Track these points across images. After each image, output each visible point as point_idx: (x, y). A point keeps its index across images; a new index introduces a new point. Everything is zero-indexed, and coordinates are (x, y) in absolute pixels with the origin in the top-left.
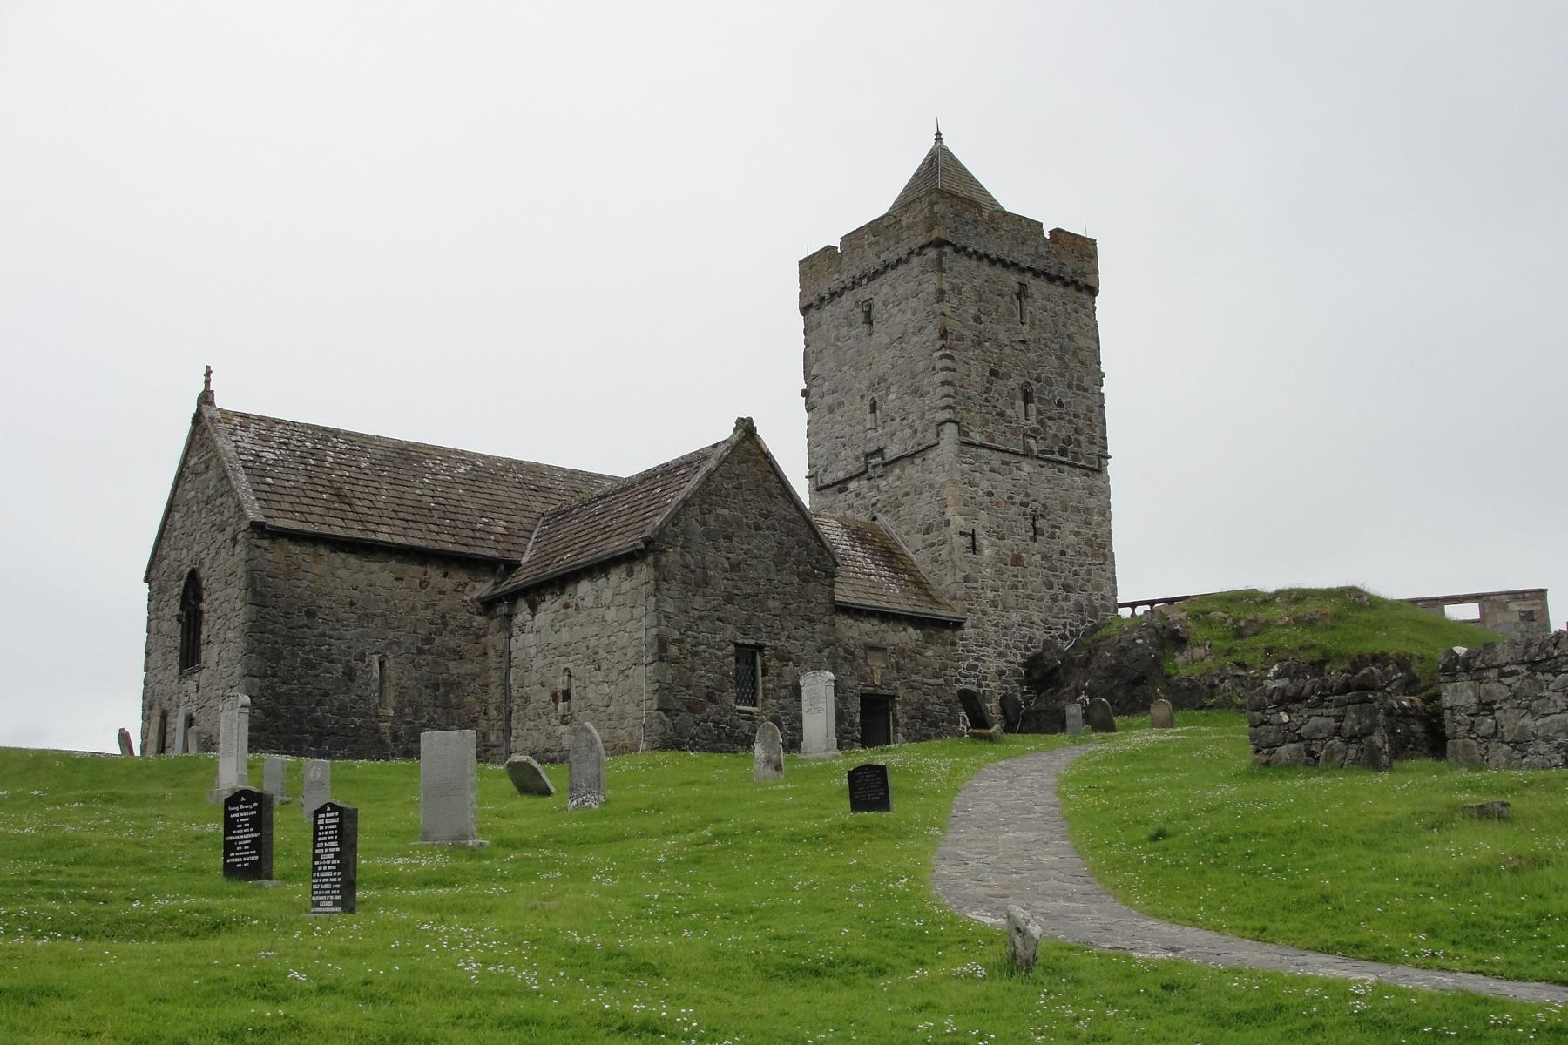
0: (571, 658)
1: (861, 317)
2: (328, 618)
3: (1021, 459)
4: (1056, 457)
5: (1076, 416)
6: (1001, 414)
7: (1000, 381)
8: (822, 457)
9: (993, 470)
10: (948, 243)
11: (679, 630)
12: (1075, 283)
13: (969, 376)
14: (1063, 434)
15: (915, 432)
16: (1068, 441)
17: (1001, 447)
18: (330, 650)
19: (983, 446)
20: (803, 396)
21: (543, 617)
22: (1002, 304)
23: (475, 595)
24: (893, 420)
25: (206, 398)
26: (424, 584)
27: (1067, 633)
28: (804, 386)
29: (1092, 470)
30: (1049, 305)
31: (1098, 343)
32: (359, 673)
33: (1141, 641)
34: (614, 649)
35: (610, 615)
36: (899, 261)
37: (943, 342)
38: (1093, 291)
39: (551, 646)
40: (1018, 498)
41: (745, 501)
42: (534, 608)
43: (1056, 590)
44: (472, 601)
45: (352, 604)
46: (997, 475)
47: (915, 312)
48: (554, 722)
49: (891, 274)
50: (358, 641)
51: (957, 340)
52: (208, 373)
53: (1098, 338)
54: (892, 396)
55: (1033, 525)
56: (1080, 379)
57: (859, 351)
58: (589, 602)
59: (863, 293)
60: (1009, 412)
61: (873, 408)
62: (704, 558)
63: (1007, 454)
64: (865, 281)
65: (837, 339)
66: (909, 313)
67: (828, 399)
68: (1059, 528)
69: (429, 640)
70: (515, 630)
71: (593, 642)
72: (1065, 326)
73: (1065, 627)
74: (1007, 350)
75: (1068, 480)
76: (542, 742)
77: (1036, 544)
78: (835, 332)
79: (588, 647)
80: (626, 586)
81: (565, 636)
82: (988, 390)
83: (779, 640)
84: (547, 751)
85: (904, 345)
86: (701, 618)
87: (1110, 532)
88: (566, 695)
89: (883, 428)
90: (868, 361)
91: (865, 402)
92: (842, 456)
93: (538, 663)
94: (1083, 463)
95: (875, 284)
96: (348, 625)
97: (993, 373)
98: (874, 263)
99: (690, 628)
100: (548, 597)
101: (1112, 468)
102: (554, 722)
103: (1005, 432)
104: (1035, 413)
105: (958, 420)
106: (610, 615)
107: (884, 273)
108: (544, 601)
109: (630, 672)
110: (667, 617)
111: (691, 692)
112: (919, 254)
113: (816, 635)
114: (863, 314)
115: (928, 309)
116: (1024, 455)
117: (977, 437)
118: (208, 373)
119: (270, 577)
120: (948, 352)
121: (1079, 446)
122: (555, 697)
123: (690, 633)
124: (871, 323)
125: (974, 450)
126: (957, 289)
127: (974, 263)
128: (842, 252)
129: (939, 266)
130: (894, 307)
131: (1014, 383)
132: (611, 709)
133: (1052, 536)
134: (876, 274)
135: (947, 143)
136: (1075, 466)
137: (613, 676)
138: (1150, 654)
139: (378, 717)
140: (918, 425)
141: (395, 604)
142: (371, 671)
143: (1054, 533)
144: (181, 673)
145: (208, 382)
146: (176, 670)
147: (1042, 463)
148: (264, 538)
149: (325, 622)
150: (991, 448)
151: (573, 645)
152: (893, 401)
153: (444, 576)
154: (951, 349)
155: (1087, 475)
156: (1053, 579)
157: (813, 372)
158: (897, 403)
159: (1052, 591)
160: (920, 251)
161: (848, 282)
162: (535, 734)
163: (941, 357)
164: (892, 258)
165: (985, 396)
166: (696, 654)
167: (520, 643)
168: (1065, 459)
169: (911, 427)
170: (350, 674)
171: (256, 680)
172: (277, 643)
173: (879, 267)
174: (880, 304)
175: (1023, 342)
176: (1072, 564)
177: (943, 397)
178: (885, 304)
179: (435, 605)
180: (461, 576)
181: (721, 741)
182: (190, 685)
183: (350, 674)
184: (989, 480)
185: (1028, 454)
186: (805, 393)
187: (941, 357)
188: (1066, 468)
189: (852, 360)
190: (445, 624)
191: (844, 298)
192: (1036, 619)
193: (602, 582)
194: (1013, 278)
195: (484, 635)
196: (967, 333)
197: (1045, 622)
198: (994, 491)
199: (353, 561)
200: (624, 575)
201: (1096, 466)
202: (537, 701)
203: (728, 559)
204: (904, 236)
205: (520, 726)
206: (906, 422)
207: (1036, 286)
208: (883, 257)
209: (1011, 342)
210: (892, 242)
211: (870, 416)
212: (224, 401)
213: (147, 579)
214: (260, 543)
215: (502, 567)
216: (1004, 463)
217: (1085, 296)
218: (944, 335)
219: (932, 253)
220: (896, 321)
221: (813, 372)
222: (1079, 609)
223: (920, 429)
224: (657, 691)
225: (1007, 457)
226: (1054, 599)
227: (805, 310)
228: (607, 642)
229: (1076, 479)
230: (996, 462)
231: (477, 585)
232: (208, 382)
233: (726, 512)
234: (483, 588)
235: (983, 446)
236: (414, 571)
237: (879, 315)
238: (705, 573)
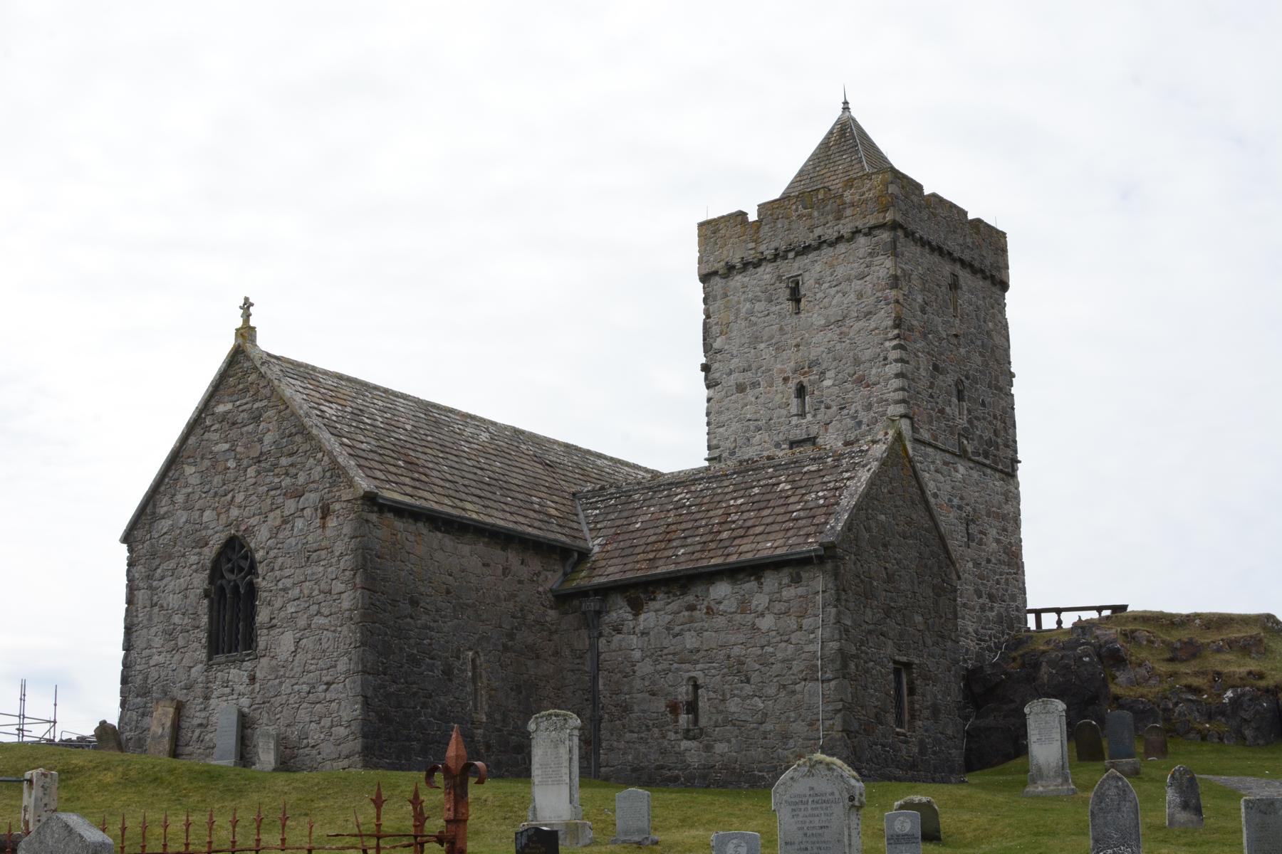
0: (699, 666)
1: (784, 293)
2: (429, 607)
3: (957, 459)
4: (981, 459)
5: (995, 417)
6: (942, 411)
7: (941, 377)
8: (727, 439)
9: (937, 471)
10: (901, 226)
11: (855, 645)
12: (992, 277)
13: (918, 369)
14: (988, 435)
15: (859, 424)
16: (990, 443)
17: (944, 447)
18: (430, 644)
19: (930, 445)
20: (702, 370)
21: (648, 618)
22: (940, 294)
23: (548, 585)
24: (828, 407)
25: (246, 333)
26: (506, 571)
27: (992, 645)
28: (703, 360)
29: (1008, 474)
30: (974, 299)
31: (1008, 340)
32: (456, 671)
33: (1087, 659)
34: (772, 660)
35: (766, 623)
36: (840, 239)
37: (896, 332)
38: (1004, 286)
39: (666, 651)
40: (956, 501)
41: (896, 506)
42: (637, 608)
43: (984, 600)
44: (545, 593)
45: (448, 592)
46: (940, 475)
47: (860, 295)
48: (671, 736)
49: (827, 252)
50: (454, 635)
51: (909, 330)
52: (247, 306)
53: (1008, 336)
54: (828, 383)
55: (967, 530)
56: (997, 379)
57: (781, 329)
58: (730, 605)
59: (792, 267)
60: (948, 409)
61: (801, 391)
62: (869, 567)
63: (947, 455)
64: (791, 255)
65: (751, 313)
66: (853, 297)
67: (737, 377)
68: (985, 535)
69: (511, 636)
70: (607, 630)
71: (736, 651)
72: (985, 322)
73: (990, 637)
74: (944, 343)
75: (991, 484)
76: (652, 757)
77: (969, 550)
78: (748, 305)
79: (729, 657)
80: (790, 592)
81: (690, 641)
82: (932, 386)
83: (922, 657)
84: (662, 767)
85: (844, 329)
86: (870, 632)
87: (1020, 541)
88: (692, 707)
89: (814, 416)
90: (794, 342)
91: (790, 384)
92: (754, 441)
93: (645, 668)
94: (1000, 467)
95: (805, 260)
96: (445, 616)
97: (936, 367)
98: (802, 235)
99: (862, 644)
100: (660, 596)
101: (1022, 472)
102: (671, 736)
103: (945, 431)
104: (965, 412)
105: (911, 415)
106: (766, 623)
107: (818, 248)
108: (654, 599)
109: (798, 687)
110: (847, 631)
111: (864, 712)
112: (866, 235)
113: (947, 653)
114: (788, 291)
115: (879, 294)
116: (959, 456)
117: (926, 436)
118: (247, 306)
119: (379, 557)
120: (902, 342)
121: (998, 449)
122: (674, 708)
123: (863, 648)
124: (798, 301)
125: (923, 448)
126: (907, 276)
127: (919, 249)
128: (759, 223)
129: (893, 251)
130: (830, 287)
131: (950, 379)
132: (768, 726)
133: (980, 543)
134: (806, 250)
135: (855, 113)
136: (996, 470)
137: (771, 691)
138: (1100, 674)
139: (473, 723)
140: (864, 417)
141: (484, 593)
142: (466, 670)
143: (981, 539)
144: (210, 659)
145: (247, 316)
146: (202, 654)
147: (972, 465)
148: (372, 512)
149: (427, 612)
150: (936, 447)
151: (703, 653)
152: (828, 387)
153: (522, 564)
154: (905, 339)
155: (1003, 480)
156: (981, 588)
157: (716, 345)
158: (836, 390)
159: (980, 600)
160: (870, 231)
161: (769, 253)
162: (643, 749)
163: (895, 348)
164: (831, 234)
165: (930, 391)
166: (867, 671)
167: (614, 645)
168: (987, 462)
169: (854, 418)
170: (448, 672)
171: (370, 677)
172: (386, 634)
173: (813, 243)
174: (812, 281)
175: (956, 336)
176: (995, 572)
177: (896, 390)
178: (819, 282)
179: (516, 596)
180: (535, 564)
181: (888, 766)
182: (237, 675)
183: (448, 672)
184: (934, 481)
185: (963, 455)
186: (706, 368)
187: (895, 348)
188: (989, 471)
189: (771, 338)
190: (524, 618)
191: (760, 270)
192: (970, 630)
193: (752, 585)
194: (947, 268)
195: (556, 632)
196: (915, 323)
197: (976, 632)
198: (938, 493)
199: (448, 541)
200: (786, 581)
201: (1008, 468)
202: (643, 711)
203: (886, 568)
204: (848, 212)
205: (615, 737)
206: (845, 412)
207: (965, 276)
208: (818, 232)
209: (948, 335)
210: (830, 217)
211: (794, 402)
212: (267, 342)
213: (128, 538)
214: (365, 515)
215: (576, 555)
216: (946, 464)
217: (996, 290)
218: (898, 324)
219: (885, 236)
220: (834, 302)
221: (716, 345)
222: (1000, 620)
223: (865, 420)
224: (840, 710)
225: (948, 457)
226: (983, 609)
227: (705, 278)
228: (759, 652)
229: (997, 483)
230: (939, 457)
231: (549, 574)
232: (247, 316)
233: (883, 517)
234: (553, 579)
235: (930, 445)
236: (498, 555)
237: (809, 294)
238: (871, 583)
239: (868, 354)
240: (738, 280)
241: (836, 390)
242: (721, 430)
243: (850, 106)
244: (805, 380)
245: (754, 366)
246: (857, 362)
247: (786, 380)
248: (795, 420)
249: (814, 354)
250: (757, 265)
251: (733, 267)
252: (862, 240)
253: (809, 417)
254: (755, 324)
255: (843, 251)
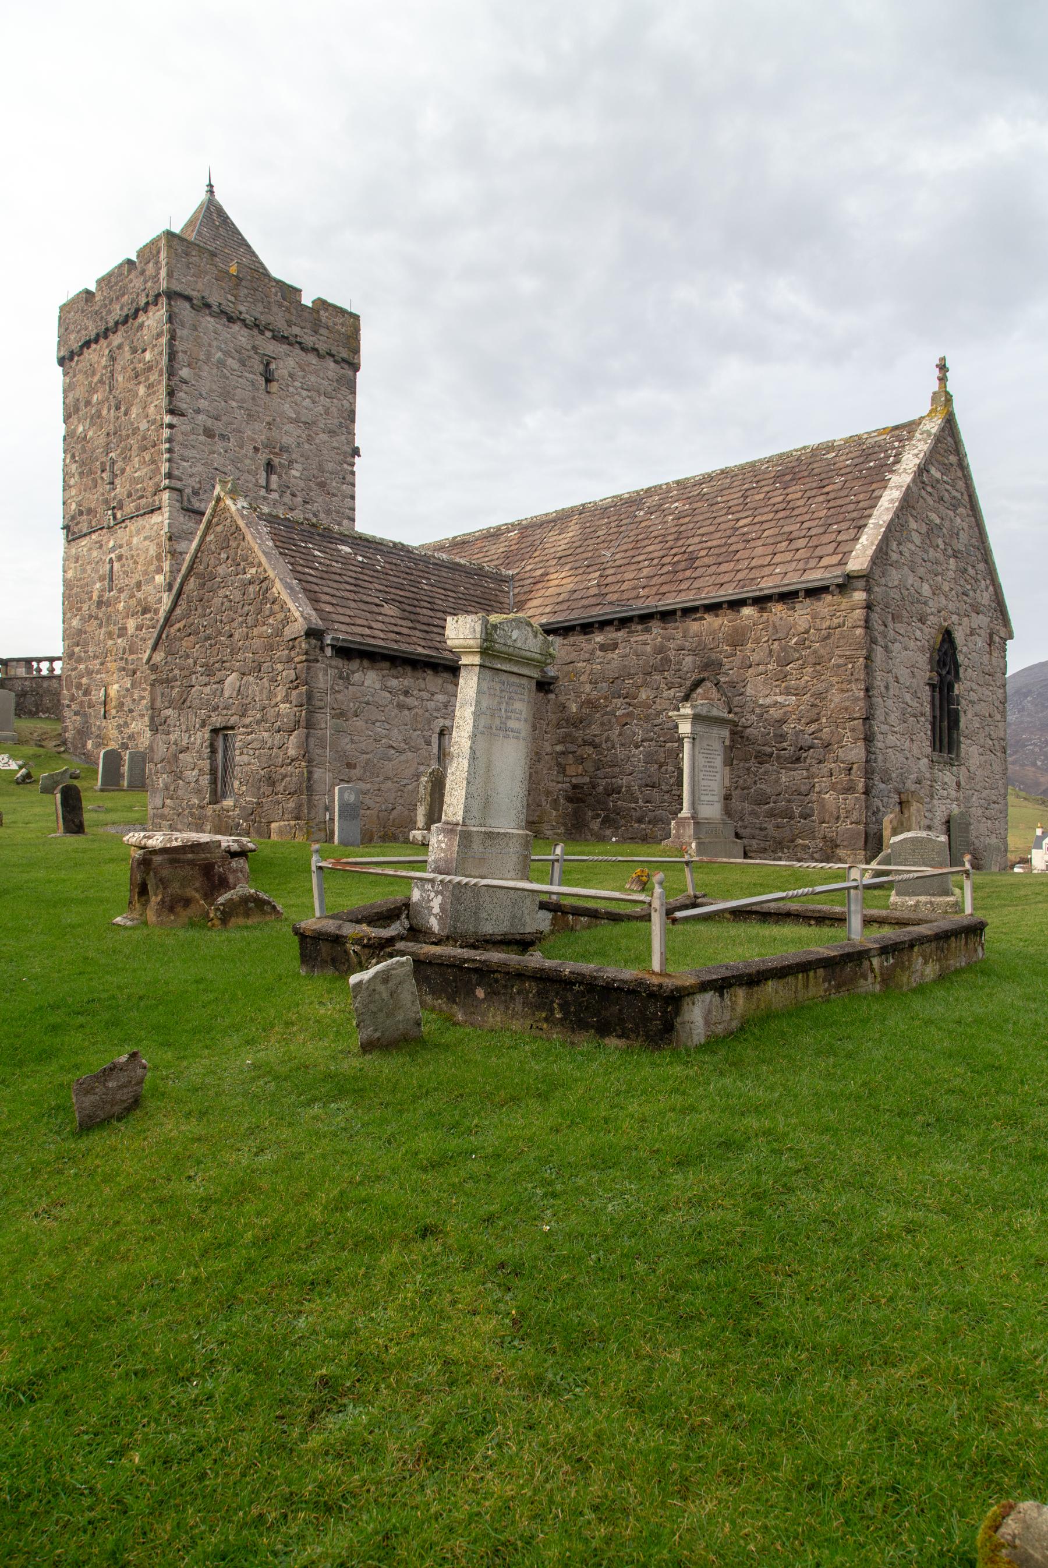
8: (191, 476)
64: (268, 334)
95: (282, 348)
112: (336, 362)
118: (943, 367)
134: (284, 339)
145: (943, 380)
152: (296, 478)
189: (243, 401)
208: (296, 330)
232: (943, 380)
239: (330, 466)
240: (209, 322)
241: (302, 484)
242: (185, 464)
243: (215, 189)
244: (276, 461)
245: (224, 418)
246: (321, 468)
247: (256, 449)
248: (263, 492)
249: (286, 440)
250: (231, 319)
251: (208, 306)
252: (332, 365)
253: (275, 496)
254: (227, 378)
255: (314, 362)
